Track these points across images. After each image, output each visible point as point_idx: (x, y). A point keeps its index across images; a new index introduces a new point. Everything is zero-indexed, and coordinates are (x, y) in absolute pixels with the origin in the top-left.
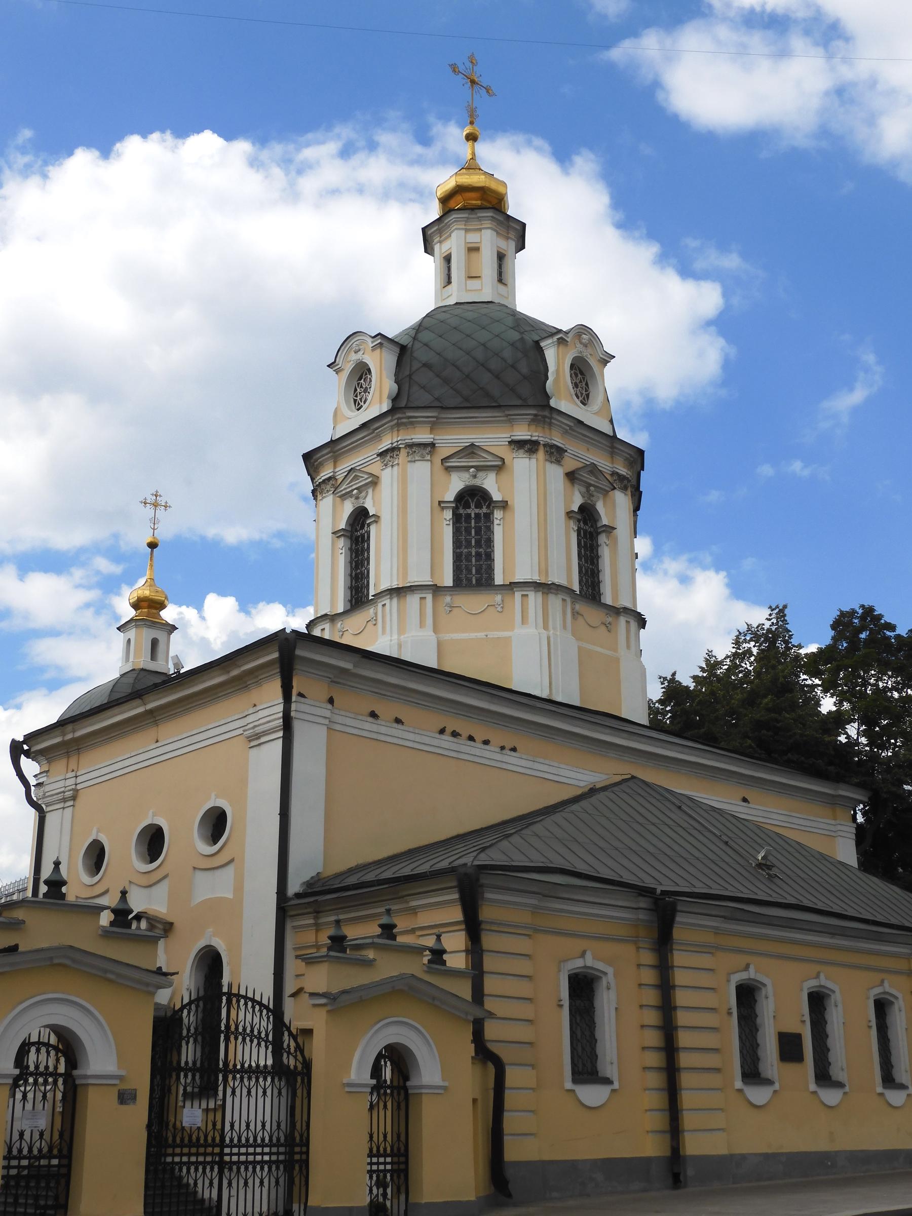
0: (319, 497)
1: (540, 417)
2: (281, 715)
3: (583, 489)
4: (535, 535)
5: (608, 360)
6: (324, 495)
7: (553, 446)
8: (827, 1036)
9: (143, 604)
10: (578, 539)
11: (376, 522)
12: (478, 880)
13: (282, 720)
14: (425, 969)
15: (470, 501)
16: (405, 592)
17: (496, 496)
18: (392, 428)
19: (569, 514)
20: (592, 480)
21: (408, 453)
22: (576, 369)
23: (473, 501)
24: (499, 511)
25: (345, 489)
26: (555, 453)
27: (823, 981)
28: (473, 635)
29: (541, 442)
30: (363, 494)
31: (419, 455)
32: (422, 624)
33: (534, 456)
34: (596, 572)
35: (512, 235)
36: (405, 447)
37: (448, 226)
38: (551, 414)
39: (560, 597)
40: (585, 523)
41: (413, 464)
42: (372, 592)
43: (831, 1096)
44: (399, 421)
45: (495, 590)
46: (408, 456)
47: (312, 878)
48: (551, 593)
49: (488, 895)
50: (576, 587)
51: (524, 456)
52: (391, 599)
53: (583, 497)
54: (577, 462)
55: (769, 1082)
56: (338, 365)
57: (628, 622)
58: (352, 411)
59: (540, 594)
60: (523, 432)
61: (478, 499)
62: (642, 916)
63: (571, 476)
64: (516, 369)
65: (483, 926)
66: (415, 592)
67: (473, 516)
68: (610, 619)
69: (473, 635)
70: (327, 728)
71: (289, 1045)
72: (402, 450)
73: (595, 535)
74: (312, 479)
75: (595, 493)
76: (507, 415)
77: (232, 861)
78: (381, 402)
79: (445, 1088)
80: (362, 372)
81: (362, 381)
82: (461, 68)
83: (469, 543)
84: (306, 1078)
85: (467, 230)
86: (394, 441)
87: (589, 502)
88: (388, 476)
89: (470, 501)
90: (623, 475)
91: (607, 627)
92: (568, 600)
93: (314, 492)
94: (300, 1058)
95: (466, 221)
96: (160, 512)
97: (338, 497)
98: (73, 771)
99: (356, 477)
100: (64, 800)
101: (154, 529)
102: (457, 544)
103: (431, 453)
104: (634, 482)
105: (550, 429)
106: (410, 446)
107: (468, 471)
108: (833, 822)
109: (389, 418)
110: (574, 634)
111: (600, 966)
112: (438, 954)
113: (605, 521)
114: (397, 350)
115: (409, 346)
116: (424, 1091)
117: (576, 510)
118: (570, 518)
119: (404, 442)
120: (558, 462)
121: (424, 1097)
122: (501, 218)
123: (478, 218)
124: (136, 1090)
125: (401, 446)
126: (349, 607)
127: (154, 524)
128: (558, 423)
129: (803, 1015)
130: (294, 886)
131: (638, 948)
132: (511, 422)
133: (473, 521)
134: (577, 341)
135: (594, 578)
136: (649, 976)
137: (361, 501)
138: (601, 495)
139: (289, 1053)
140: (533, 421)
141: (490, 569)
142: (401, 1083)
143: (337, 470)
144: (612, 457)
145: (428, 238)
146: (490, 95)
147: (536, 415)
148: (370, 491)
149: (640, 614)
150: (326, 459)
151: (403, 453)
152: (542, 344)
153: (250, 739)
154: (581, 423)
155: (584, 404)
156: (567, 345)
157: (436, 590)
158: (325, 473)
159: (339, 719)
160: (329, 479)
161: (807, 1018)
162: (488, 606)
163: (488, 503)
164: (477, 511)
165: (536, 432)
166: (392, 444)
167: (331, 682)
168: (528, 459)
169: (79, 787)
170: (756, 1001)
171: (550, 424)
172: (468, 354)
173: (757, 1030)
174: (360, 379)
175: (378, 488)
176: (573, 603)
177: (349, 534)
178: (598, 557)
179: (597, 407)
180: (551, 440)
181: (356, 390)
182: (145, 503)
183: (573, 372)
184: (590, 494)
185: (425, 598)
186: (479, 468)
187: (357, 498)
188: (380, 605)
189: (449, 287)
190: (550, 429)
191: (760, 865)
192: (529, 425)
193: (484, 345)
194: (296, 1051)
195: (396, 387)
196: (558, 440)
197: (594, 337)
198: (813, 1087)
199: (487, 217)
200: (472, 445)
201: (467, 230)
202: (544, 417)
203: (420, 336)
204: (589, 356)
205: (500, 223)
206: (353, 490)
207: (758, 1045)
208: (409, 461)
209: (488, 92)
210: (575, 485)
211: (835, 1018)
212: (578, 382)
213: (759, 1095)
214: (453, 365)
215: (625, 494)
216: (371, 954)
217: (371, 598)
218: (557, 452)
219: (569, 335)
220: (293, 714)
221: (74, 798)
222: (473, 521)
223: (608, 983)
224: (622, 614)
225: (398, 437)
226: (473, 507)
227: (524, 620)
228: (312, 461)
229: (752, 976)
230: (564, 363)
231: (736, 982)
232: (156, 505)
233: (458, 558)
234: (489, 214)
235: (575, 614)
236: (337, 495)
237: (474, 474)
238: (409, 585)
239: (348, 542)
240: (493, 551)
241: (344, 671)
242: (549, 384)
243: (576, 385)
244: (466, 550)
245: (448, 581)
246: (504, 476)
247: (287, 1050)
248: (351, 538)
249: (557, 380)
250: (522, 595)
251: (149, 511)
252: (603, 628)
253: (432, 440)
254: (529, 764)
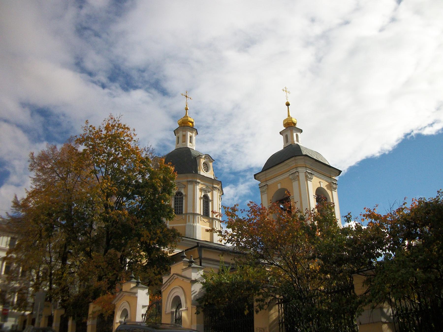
17: (184, 194)
40: (206, 199)
50: (202, 214)
83: (178, 204)
85: (183, 131)
117: (202, 197)
141: (182, 210)
155: (206, 172)
189: (178, 144)
201: (183, 131)
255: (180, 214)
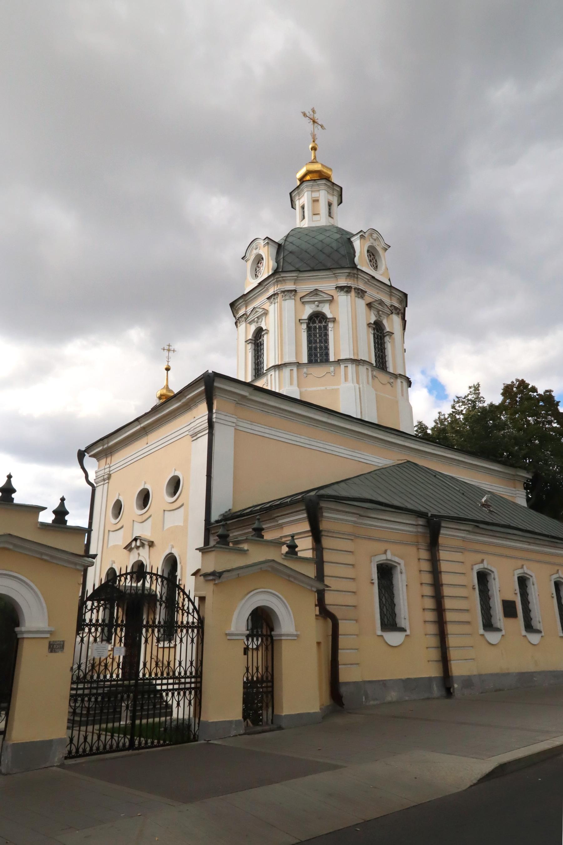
0: (239, 325)
1: (351, 274)
2: (207, 421)
3: (376, 313)
4: (351, 336)
5: (387, 248)
6: (241, 324)
7: (359, 289)
8: (529, 603)
9: (162, 397)
10: (374, 339)
11: (267, 333)
12: (318, 504)
13: (207, 424)
14: (283, 557)
15: (316, 319)
16: (282, 367)
17: (329, 315)
18: (274, 284)
19: (369, 325)
20: (380, 307)
21: (283, 296)
22: (370, 253)
23: (317, 319)
24: (331, 324)
25: (251, 318)
26: (360, 293)
27: (526, 570)
28: (319, 388)
29: (353, 287)
30: (260, 320)
31: (288, 296)
32: (291, 384)
33: (349, 294)
34: (384, 356)
35: (335, 193)
36: (281, 293)
37: (302, 190)
38: (358, 272)
39: (365, 367)
40: (378, 331)
41: (285, 301)
42: (265, 368)
43: (534, 638)
44: (278, 279)
45: (330, 364)
46: (282, 297)
47: (226, 512)
48: (360, 365)
49: (325, 514)
50: (374, 362)
51: (344, 294)
52: (275, 371)
53: (376, 317)
54: (371, 299)
55: (498, 630)
56: (247, 257)
57: (402, 382)
58: (254, 279)
59: (354, 365)
60: (343, 282)
61: (320, 319)
62: (420, 529)
63: (369, 305)
64: (338, 252)
65: (323, 533)
66: (288, 366)
67: (317, 327)
68: (392, 380)
69: (319, 388)
70: (235, 429)
71: (188, 608)
72: (279, 295)
73: (383, 338)
74: (235, 316)
75: (382, 315)
76: (334, 274)
77: (182, 505)
78: (268, 272)
79: (297, 636)
80: (259, 259)
81: (259, 264)
82: (308, 115)
83: (316, 342)
84: (200, 630)
85: (312, 191)
86: (275, 290)
87: (379, 319)
88: (272, 308)
89: (316, 319)
90: (397, 307)
91: (391, 384)
92: (370, 369)
93: (236, 323)
94: (196, 615)
95: (312, 187)
96: (171, 353)
97: (248, 323)
98: (108, 464)
99: (257, 312)
100: (104, 480)
101: (168, 362)
102: (309, 342)
103: (295, 295)
104: (402, 311)
105: (357, 281)
106: (283, 292)
107: (314, 303)
108: (514, 489)
109: (272, 279)
110: (373, 387)
111: (396, 559)
112: (292, 547)
113: (388, 329)
114: (277, 246)
115: (283, 244)
116: (283, 638)
117: (373, 323)
118: (369, 327)
119: (280, 290)
120: (362, 297)
121: (283, 641)
122: (329, 184)
123: (318, 184)
124: (64, 641)
125: (279, 292)
126: (254, 378)
127: (168, 359)
128: (362, 278)
129: (516, 590)
130: (215, 517)
131: (418, 549)
132: (336, 278)
133: (318, 330)
134: (370, 237)
135: (383, 360)
136: (426, 566)
137: (259, 323)
138: (385, 317)
139: (188, 613)
140: (348, 276)
141: (327, 355)
142: (269, 633)
143: (247, 310)
144: (391, 298)
145: (293, 199)
146: (323, 129)
147: (349, 273)
148: (264, 318)
149: (408, 378)
150: (241, 305)
151: (280, 296)
152: (352, 239)
153: (192, 436)
154: (373, 277)
156: (365, 239)
157: (299, 365)
158: (241, 312)
159: (241, 424)
160: (243, 315)
161: (518, 591)
162: (327, 373)
163: (325, 321)
164: (320, 324)
165: (349, 282)
166: (274, 292)
167: (238, 403)
168: (346, 296)
169: (111, 473)
170: (488, 581)
171: (357, 278)
172: (313, 246)
173: (490, 599)
174: (258, 263)
175: (267, 317)
176: (372, 371)
177: (253, 342)
178: (385, 349)
179: (382, 272)
180: (358, 286)
181: (256, 269)
182: (164, 349)
183: (368, 254)
184: (380, 316)
185: (293, 370)
186: (320, 302)
187: (257, 322)
188: (269, 375)
189: (304, 221)
190: (357, 281)
191: (483, 505)
192: (346, 278)
193: (321, 241)
194: (193, 612)
195: (276, 264)
196: (362, 287)
197: (379, 236)
198: (524, 633)
199: (323, 183)
200: (316, 289)
202: (354, 274)
203: (288, 239)
204: (377, 245)
205: (329, 187)
206: (255, 319)
207: (490, 607)
208: (283, 300)
209: (322, 127)
210: (372, 310)
211: (533, 591)
212: (371, 259)
213: (493, 637)
214: (306, 252)
215: (398, 317)
216: (245, 546)
217: (265, 372)
218: (362, 292)
219: (366, 233)
220: (214, 420)
221: (109, 478)
222: (318, 330)
223: (401, 569)
224: (399, 378)
225: (277, 287)
226: (317, 322)
227: (346, 379)
228: (235, 307)
229: (486, 567)
230: (364, 249)
231: (477, 570)
232: (169, 350)
233: (310, 349)
234: (324, 182)
235: (374, 377)
236: (247, 322)
237: (317, 305)
238: (284, 363)
239: (253, 346)
240: (329, 345)
241: (244, 397)
242: (356, 260)
243: (370, 261)
244: (314, 345)
245: (305, 360)
246: (333, 305)
247: (187, 611)
248: (255, 344)
249: (359, 257)
250: (345, 367)
251: (166, 353)
252: (389, 385)
253: (295, 288)
254: (350, 453)
255: (321, 361)
